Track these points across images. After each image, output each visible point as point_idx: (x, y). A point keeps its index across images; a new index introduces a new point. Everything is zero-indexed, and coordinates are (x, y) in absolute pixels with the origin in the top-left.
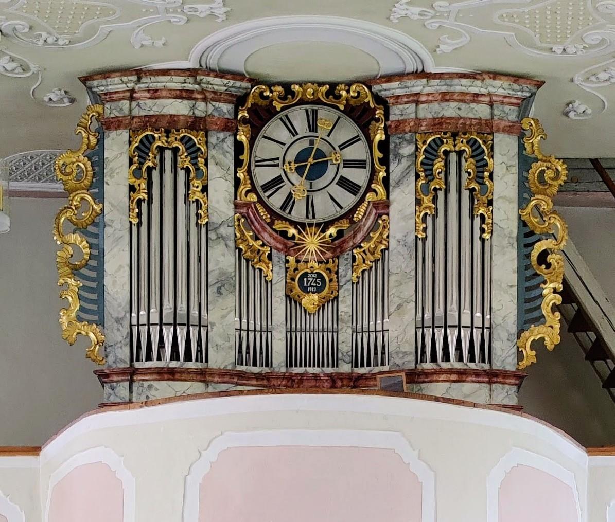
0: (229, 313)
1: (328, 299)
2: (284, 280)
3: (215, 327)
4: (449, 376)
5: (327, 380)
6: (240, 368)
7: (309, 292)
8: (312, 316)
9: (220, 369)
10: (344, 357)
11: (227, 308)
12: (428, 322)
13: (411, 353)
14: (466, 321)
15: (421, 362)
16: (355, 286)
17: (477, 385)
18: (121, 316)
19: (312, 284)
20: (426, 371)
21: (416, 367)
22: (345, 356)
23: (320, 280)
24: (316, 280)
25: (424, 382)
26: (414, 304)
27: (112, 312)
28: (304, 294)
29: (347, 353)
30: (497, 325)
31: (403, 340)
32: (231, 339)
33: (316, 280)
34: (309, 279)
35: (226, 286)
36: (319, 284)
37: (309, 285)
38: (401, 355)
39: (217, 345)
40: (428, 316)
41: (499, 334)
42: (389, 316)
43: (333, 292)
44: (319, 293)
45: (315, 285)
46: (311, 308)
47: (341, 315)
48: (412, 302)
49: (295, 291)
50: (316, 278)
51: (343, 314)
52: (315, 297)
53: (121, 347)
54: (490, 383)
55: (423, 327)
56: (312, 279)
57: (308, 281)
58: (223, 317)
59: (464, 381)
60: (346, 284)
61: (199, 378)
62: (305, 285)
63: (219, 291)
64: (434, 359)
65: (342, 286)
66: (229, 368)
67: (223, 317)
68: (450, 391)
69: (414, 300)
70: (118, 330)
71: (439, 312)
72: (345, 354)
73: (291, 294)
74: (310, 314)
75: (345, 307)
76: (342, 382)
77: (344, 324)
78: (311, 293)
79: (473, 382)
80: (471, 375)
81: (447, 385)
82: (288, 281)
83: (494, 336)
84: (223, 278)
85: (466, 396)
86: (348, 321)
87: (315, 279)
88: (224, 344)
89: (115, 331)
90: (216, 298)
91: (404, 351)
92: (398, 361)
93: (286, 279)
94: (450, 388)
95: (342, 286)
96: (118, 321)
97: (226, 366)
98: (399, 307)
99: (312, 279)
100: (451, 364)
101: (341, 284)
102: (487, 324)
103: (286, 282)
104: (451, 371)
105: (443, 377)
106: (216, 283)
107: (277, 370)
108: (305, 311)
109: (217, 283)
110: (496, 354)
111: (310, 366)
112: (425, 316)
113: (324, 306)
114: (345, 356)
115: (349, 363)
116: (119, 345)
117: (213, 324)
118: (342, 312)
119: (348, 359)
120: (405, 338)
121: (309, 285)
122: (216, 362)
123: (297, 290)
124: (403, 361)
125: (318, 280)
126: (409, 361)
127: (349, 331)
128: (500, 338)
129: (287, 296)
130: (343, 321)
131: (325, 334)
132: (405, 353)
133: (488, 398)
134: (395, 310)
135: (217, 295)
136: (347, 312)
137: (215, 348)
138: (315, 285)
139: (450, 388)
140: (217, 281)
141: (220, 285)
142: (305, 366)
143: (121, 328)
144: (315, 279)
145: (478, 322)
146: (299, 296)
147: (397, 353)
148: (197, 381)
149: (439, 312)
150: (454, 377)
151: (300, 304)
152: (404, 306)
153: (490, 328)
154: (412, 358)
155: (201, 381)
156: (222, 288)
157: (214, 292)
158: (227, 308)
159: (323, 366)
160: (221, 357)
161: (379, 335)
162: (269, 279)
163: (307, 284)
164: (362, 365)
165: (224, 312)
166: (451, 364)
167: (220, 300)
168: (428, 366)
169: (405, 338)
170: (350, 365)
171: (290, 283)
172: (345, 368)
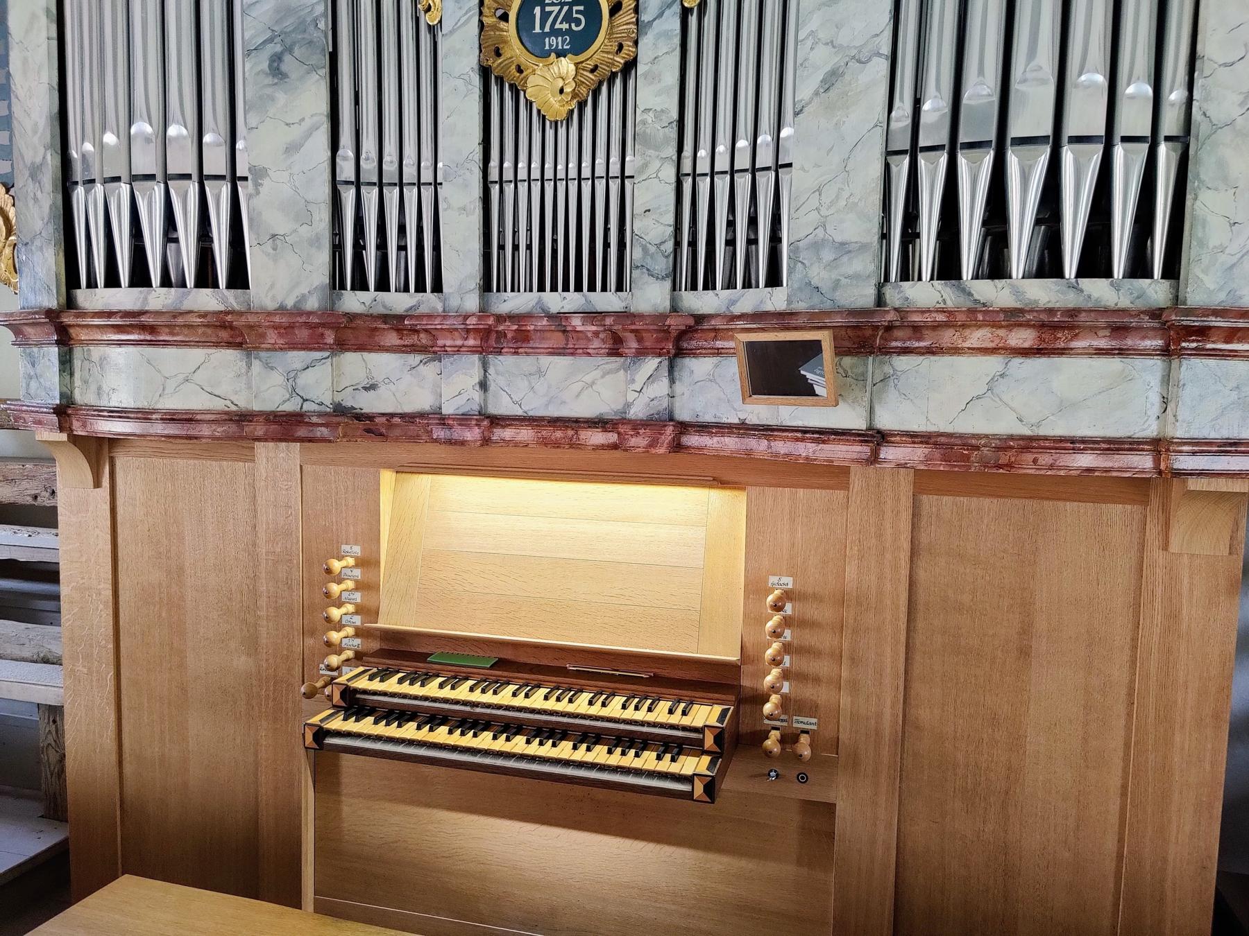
0: (309, 134)
1: (605, 71)
2: (476, 19)
3: (266, 182)
4: (1002, 332)
5: (596, 334)
6: (354, 302)
7: (546, 55)
8: (550, 133)
9: (282, 310)
10: (649, 260)
11: (303, 119)
12: (934, 129)
13: (864, 247)
14: (1086, 115)
15: (905, 275)
16: (693, 20)
17: (1115, 363)
18: (38, 160)
19: (557, 26)
20: (916, 318)
21: (880, 300)
22: (652, 256)
23: (582, 8)
24: (570, 10)
25: (906, 351)
26: (883, 66)
27: (24, 151)
28: (533, 59)
29: (658, 246)
30: (1215, 128)
31: (837, 197)
32: (316, 217)
33: (570, 10)
34: (548, 9)
35: (297, 52)
36: (578, 22)
37: (547, 29)
38: (827, 255)
39: (274, 236)
40: (935, 107)
41: (1222, 164)
42: (796, 114)
43: (621, 47)
44: (576, 54)
45: (565, 26)
46: (557, 107)
47: (644, 122)
48: (876, 59)
49: (506, 53)
50: (571, 5)
51: (649, 117)
52: (566, 66)
53: (41, 249)
54: (1166, 352)
55: (914, 151)
56: (557, 8)
57: (545, 16)
58: (292, 149)
59: (1062, 352)
60: (661, 15)
61: (224, 335)
62: (537, 30)
63: (276, 69)
64: (948, 268)
65: (650, 23)
66: (313, 304)
67: (292, 149)
68: (1001, 386)
69: (886, 49)
70: (36, 199)
71: (981, 89)
72: (652, 249)
73: (495, 63)
74: (556, 124)
75: (655, 94)
76: (640, 340)
77: (651, 152)
78: (553, 55)
79: (1100, 352)
80: (1094, 330)
81: (993, 364)
82: (486, 20)
83: (1203, 170)
84: (289, 23)
85: (1065, 407)
86: (666, 140)
87: (566, 8)
88: (295, 231)
89: (31, 203)
90: (269, 91)
91: (838, 239)
92: (819, 274)
93: (481, 13)
94: (1002, 376)
95: (650, 23)
96: (35, 172)
97: (303, 298)
98: (831, 80)
99: (557, 8)
100: (1013, 286)
101: (645, 17)
102: (1171, 123)
103: (482, 26)
104: (1013, 317)
105: (978, 337)
106: (264, 42)
107: (454, 302)
108: (543, 119)
109: (270, 40)
110: (1202, 244)
111: (554, 288)
112: (926, 107)
113: (596, 93)
114: (652, 256)
115: (663, 278)
116: (38, 243)
117: (259, 173)
118: (647, 110)
119: (662, 265)
120: (845, 194)
121: (547, 29)
122: (272, 286)
123: (515, 50)
124: (834, 275)
125: (575, 8)
126: (856, 277)
127: (669, 173)
128: (1225, 179)
129: (485, 72)
130: (648, 142)
131: (600, 186)
132: (843, 248)
133: (1156, 409)
134: (817, 94)
135: (269, 80)
136: (662, 111)
137: (268, 247)
138: (565, 26)
139: (1002, 376)
140: (268, 34)
141: (278, 48)
142: (541, 288)
143: (39, 194)
144: (566, 8)
145: (1135, 119)
146: (520, 70)
147: (817, 246)
148: (217, 345)
149: (981, 89)
150: (1022, 337)
151: (529, 104)
152: (847, 77)
153: (1183, 140)
154: (866, 265)
155: (230, 345)
156: (287, 58)
157: (262, 71)
158: (303, 119)
159: (592, 288)
160: (288, 273)
161: (766, 182)
162: (428, 19)
163: (542, 26)
164: (709, 284)
165: (296, 133)
166: (1013, 286)
167: (281, 97)
168: (925, 293)
169: (845, 194)
170: (668, 284)
171: (495, 28)
172: (650, 296)
